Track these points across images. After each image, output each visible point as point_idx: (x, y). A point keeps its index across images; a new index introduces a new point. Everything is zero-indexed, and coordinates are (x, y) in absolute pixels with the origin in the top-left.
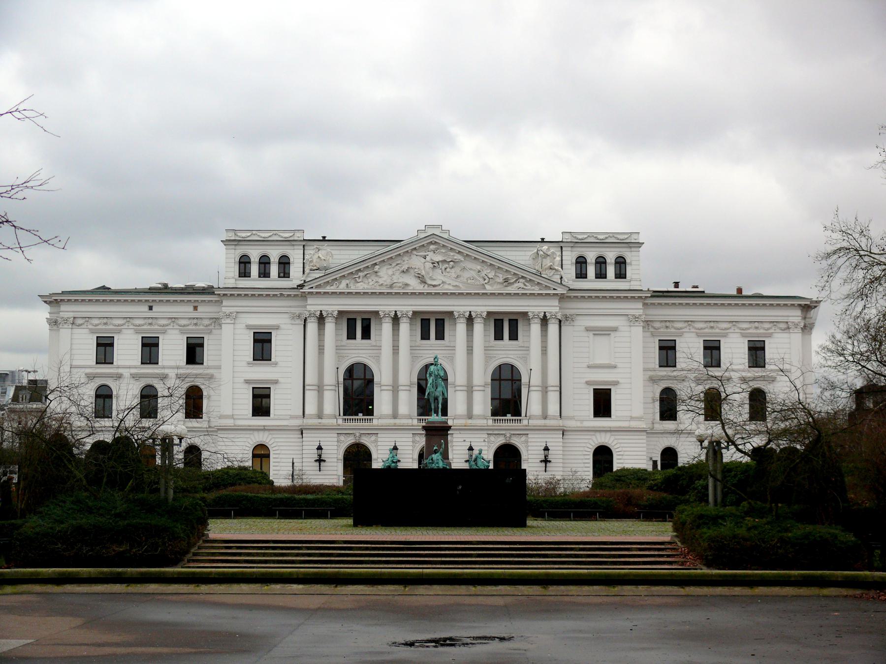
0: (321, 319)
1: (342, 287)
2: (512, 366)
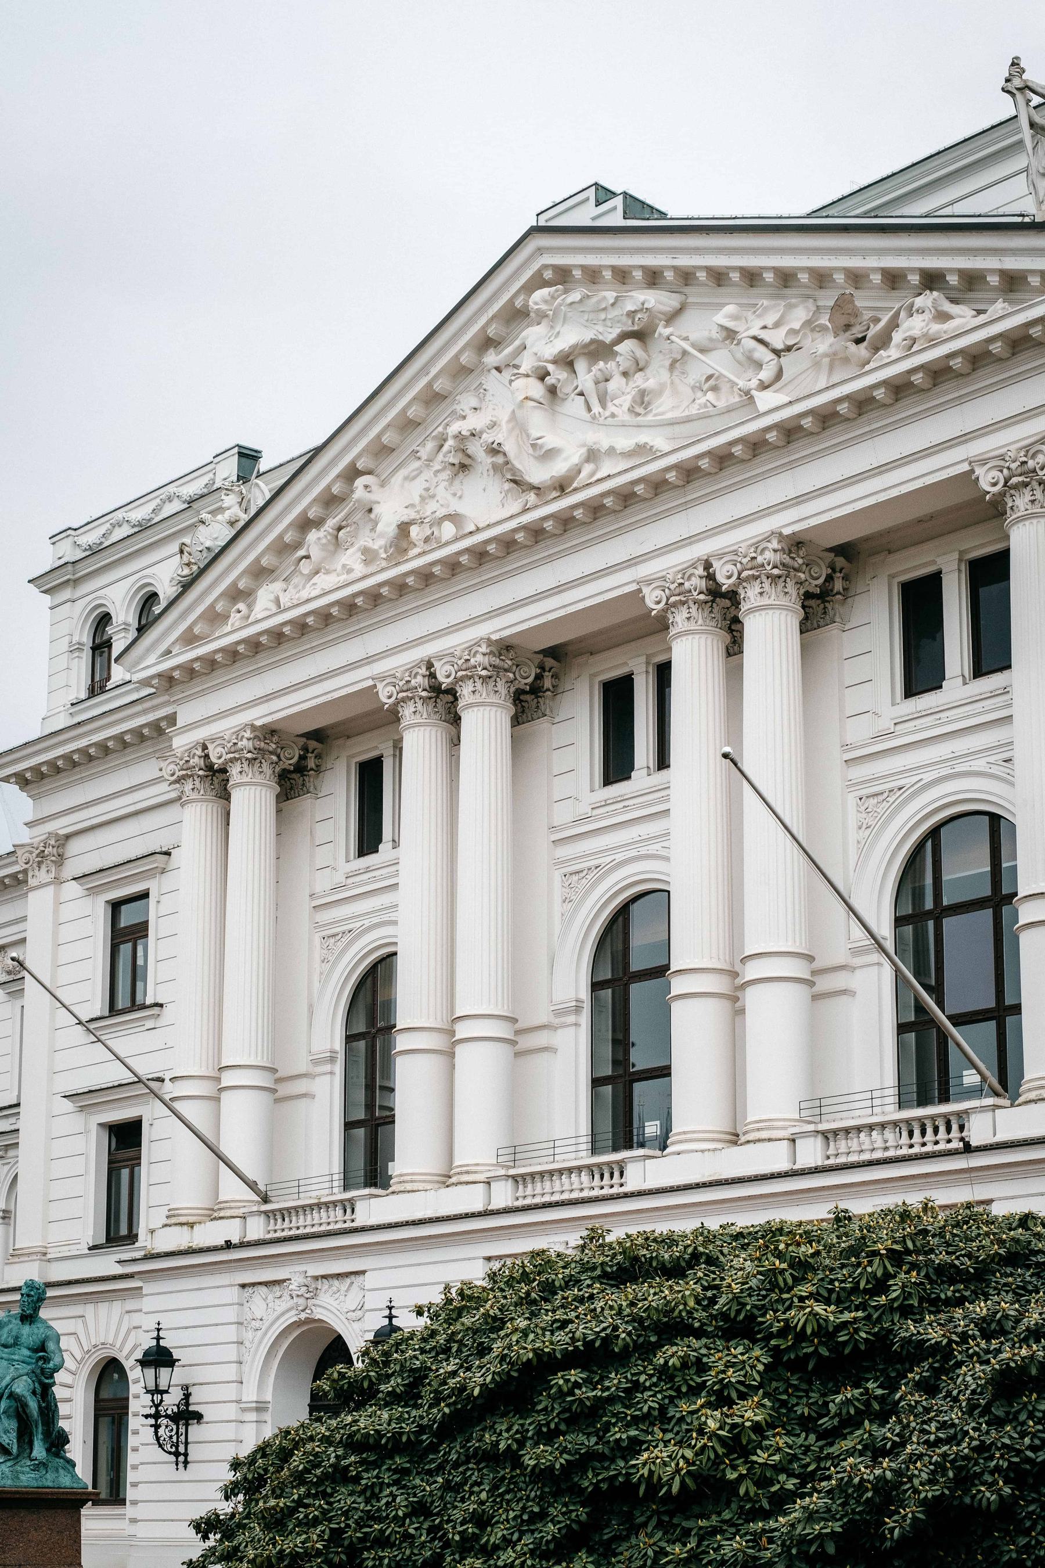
0: (216, 778)
1: (270, 606)
2: (995, 819)
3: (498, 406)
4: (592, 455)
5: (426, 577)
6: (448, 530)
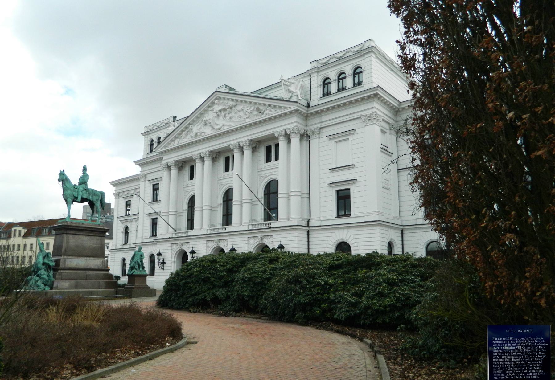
0: (169, 168)
3: (210, 116)
4: (223, 125)
5: (200, 141)
6: (203, 134)
